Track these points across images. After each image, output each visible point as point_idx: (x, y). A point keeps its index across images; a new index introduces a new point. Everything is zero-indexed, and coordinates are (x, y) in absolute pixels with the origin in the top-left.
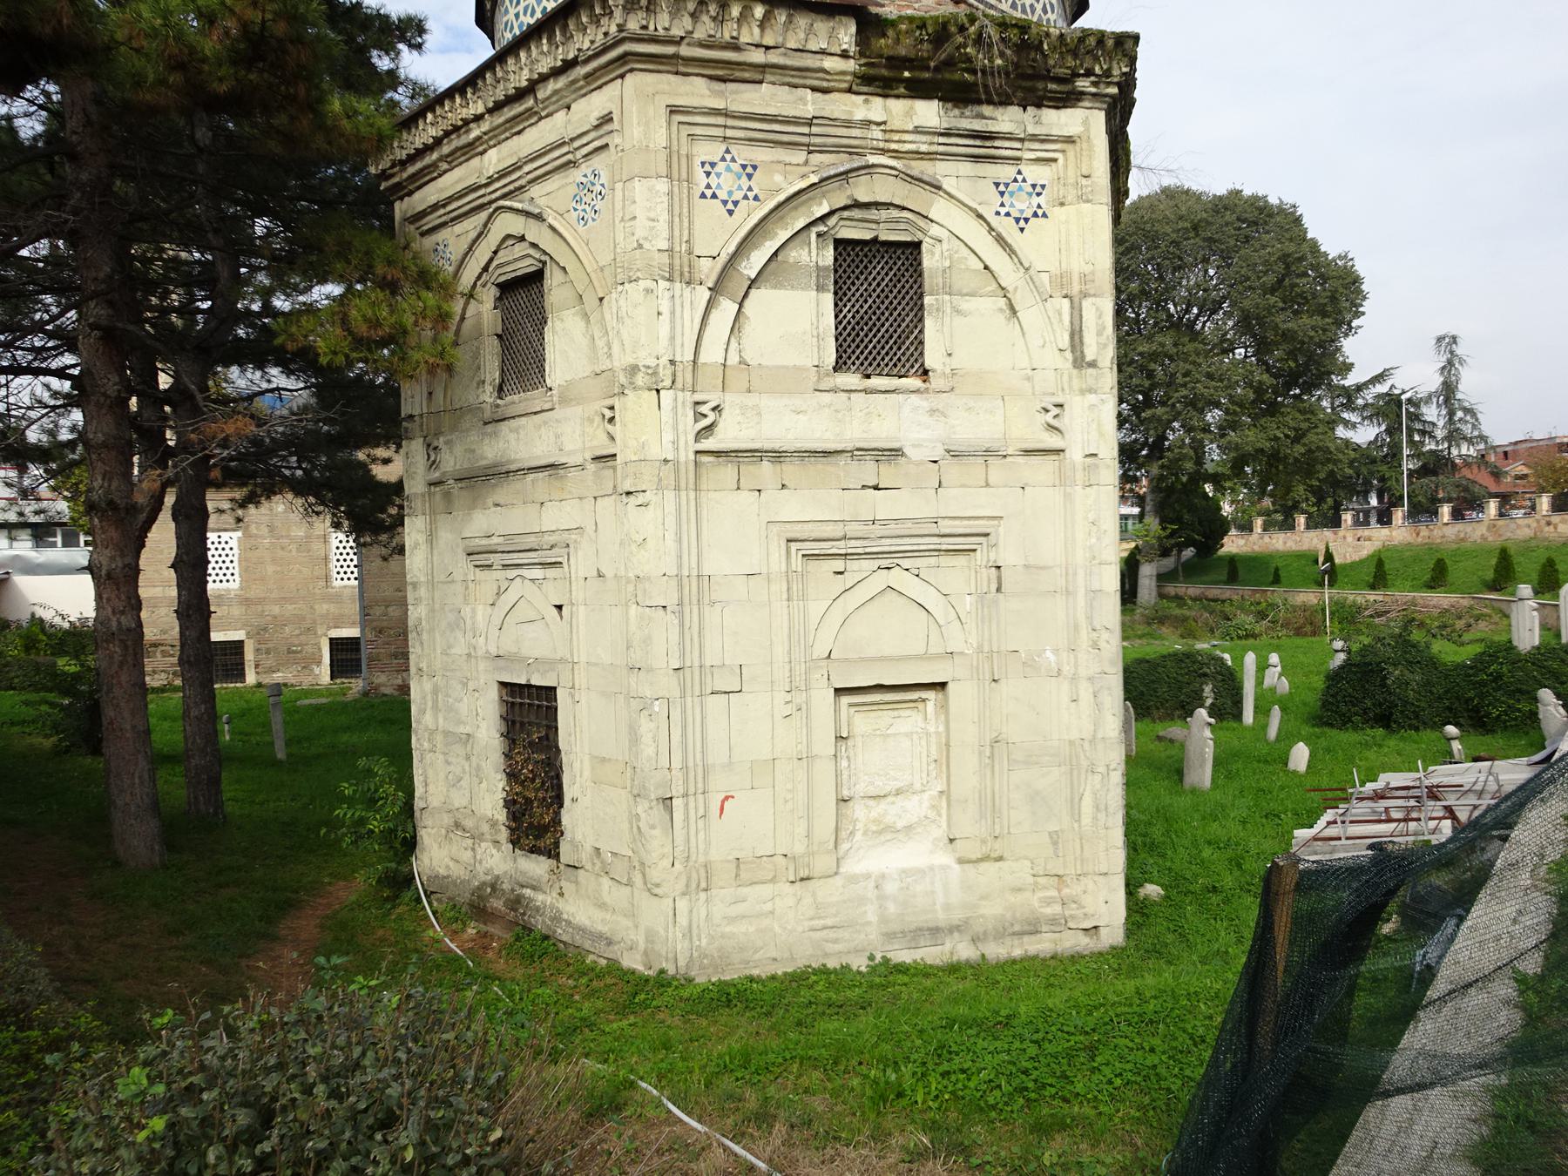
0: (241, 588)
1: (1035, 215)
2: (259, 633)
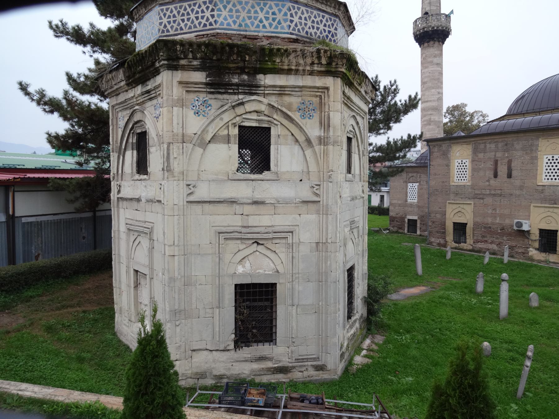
0: (418, 202)
2: (421, 217)
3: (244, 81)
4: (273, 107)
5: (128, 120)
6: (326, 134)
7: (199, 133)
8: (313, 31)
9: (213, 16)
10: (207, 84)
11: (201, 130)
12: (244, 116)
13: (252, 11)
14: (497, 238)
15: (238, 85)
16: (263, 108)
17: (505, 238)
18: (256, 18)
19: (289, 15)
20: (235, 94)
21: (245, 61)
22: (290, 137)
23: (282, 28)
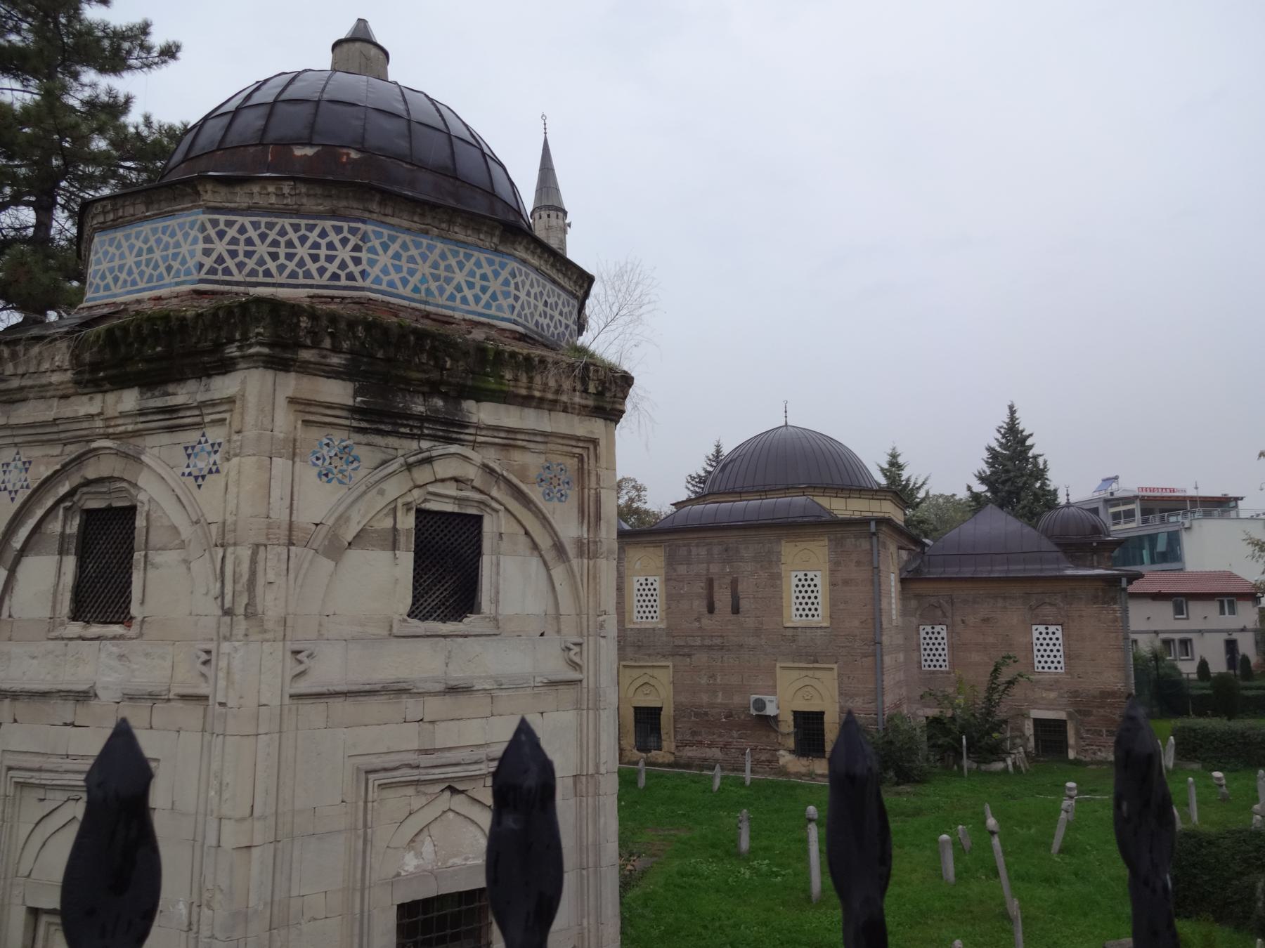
1: (210, 472)
3: (437, 411)
4: (492, 471)
5: (56, 472)
6: (591, 535)
7: (330, 522)
8: (542, 320)
9: (357, 261)
10: (353, 410)
11: (336, 515)
12: (431, 488)
13: (442, 265)
14: (720, 735)
15: (422, 419)
16: (471, 472)
17: (735, 734)
18: (448, 280)
19: (512, 286)
20: (412, 436)
21: (443, 368)
22: (522, 539)
23: (500, 308)
